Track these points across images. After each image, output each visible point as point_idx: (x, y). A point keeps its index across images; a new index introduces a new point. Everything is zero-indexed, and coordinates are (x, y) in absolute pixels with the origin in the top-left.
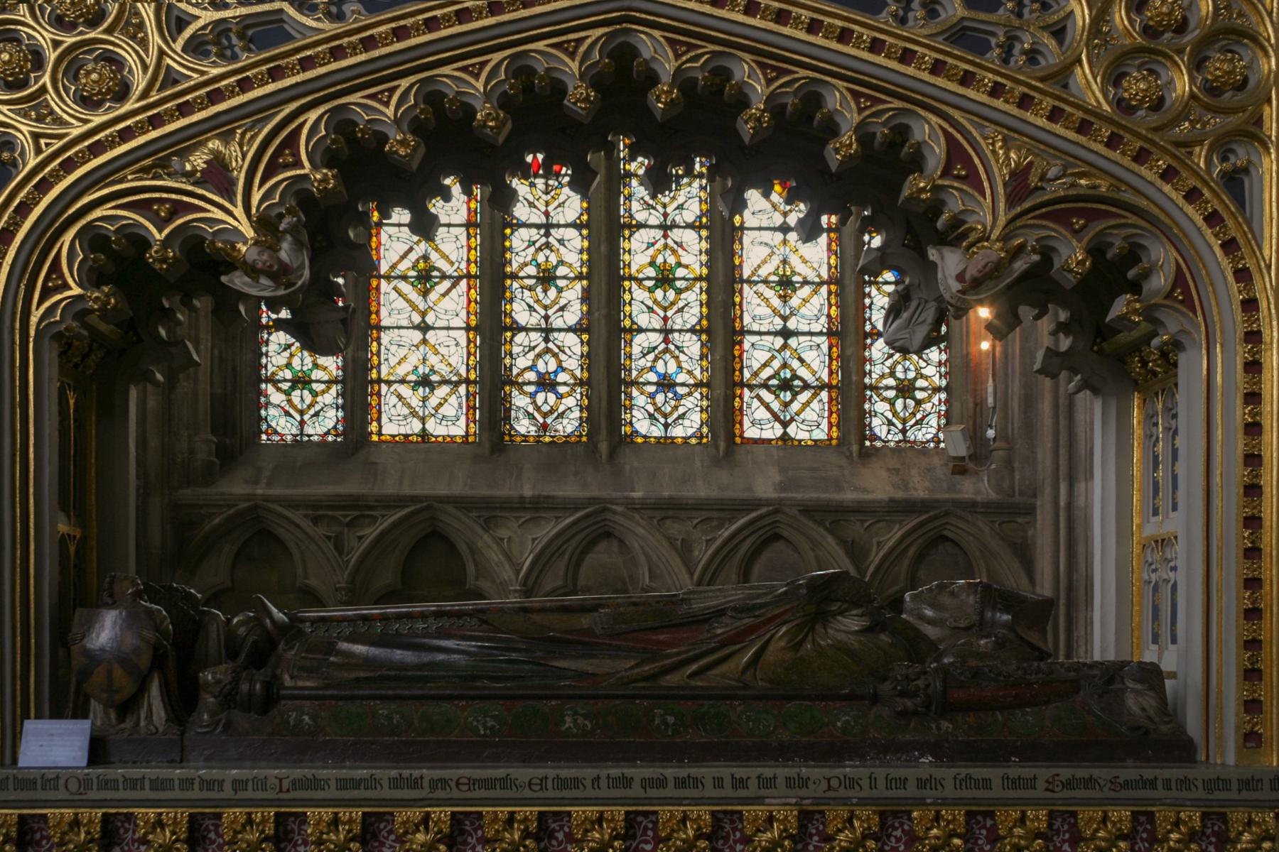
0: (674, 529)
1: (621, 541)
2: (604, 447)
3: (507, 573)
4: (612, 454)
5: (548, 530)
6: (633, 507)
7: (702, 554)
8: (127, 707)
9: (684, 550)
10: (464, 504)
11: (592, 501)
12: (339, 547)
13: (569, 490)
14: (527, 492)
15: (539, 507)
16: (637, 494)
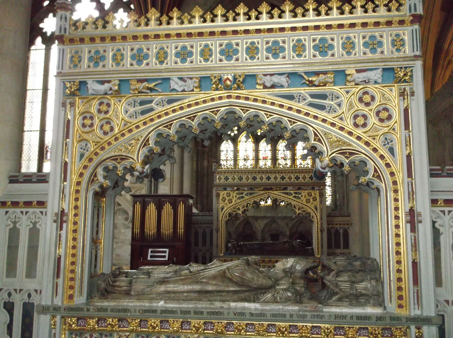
0: (285, 221)
1: (277, 224)
2: (274, 207)
3: (259, 228)
4: (276, 207)
5: (265, 221)
6: (279, 217)
7: (290, 225)
8: (231, 251)
9: (287, 224)
10: (253, 217)
11: (272, 217)
12: (233, 224)
13: (269, 215)
14: (262, 215)
15: (264, 217)
16: (280, 215)
